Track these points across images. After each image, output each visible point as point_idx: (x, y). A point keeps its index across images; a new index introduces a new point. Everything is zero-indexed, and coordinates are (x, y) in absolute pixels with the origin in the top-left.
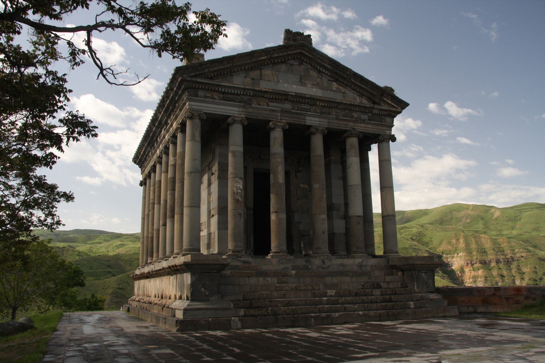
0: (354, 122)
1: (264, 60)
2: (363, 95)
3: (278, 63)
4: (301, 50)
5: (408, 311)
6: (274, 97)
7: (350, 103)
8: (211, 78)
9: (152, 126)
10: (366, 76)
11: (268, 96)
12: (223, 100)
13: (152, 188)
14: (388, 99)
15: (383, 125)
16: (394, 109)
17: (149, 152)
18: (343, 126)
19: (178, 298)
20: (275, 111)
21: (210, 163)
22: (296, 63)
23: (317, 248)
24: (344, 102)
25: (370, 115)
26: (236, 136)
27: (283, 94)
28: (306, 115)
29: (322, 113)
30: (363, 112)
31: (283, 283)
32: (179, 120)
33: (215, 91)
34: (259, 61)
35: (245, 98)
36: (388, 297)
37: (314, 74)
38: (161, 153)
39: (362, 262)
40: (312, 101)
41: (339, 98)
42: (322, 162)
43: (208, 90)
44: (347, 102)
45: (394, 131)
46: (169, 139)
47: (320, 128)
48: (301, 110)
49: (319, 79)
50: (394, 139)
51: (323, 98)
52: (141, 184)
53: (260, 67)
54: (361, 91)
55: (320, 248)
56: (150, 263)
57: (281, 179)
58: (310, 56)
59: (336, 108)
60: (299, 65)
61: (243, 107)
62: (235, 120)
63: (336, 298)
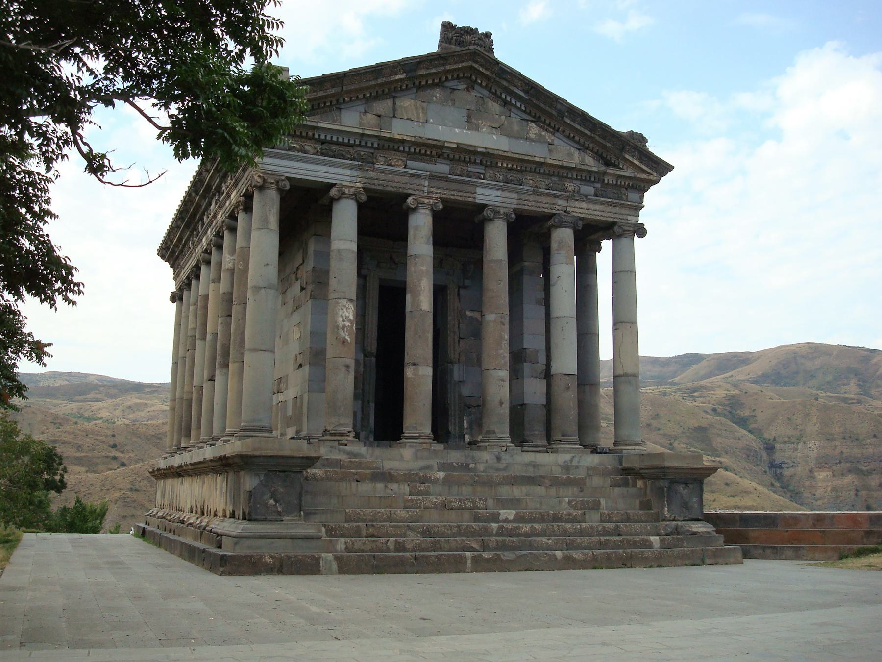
0: (567, 199)
1: (401, 80)
3: (428, 86)
4: (470, 63)
5: (647, 552)
6: (417, 151)
7: (560, 163)
9: (193, 194)
10: (593, 114)
11: (407, 149)
12: (323, 154)
13: (192, 308)
14: (633, 156)
15: (622, 206)
16: (644, 176)
17: (188, 240)
18: (547, 206)
19: (228, 516)
20: (419, 176)
21: (298, 268)
22: (462, 86)
23: (488, 432)
24: (550, 161)
25: (598, 185)
26: (345, 222)
27: (434, 146)
28: (476, 185)
29: (507, 182)
30: (585, 180)
31: (420, 493)
32: (242, 187)
33: (307, 137)
34: (391, 83)
35: (363, 152)
36: (611, 526)
37: (494, 107)
38: (209, 244)
39: (571, 461)
41: (539, 153)
42: (504, 273)
45: (643, 217)
46: (223, 222)
47: (502, 211)
48: (468, 176)
49: (503, 117)
50: (641, 231)
51: (509, 155)
52: (174, 298)
53: (394, 94)
54: (582, 140)
55: (494, 432)
56: (185, 449)
57: (425, 302)
58: (488, 73)
59: (535, 172)
61: (360, 168)
62: (344, 193)
63: (515, 525)
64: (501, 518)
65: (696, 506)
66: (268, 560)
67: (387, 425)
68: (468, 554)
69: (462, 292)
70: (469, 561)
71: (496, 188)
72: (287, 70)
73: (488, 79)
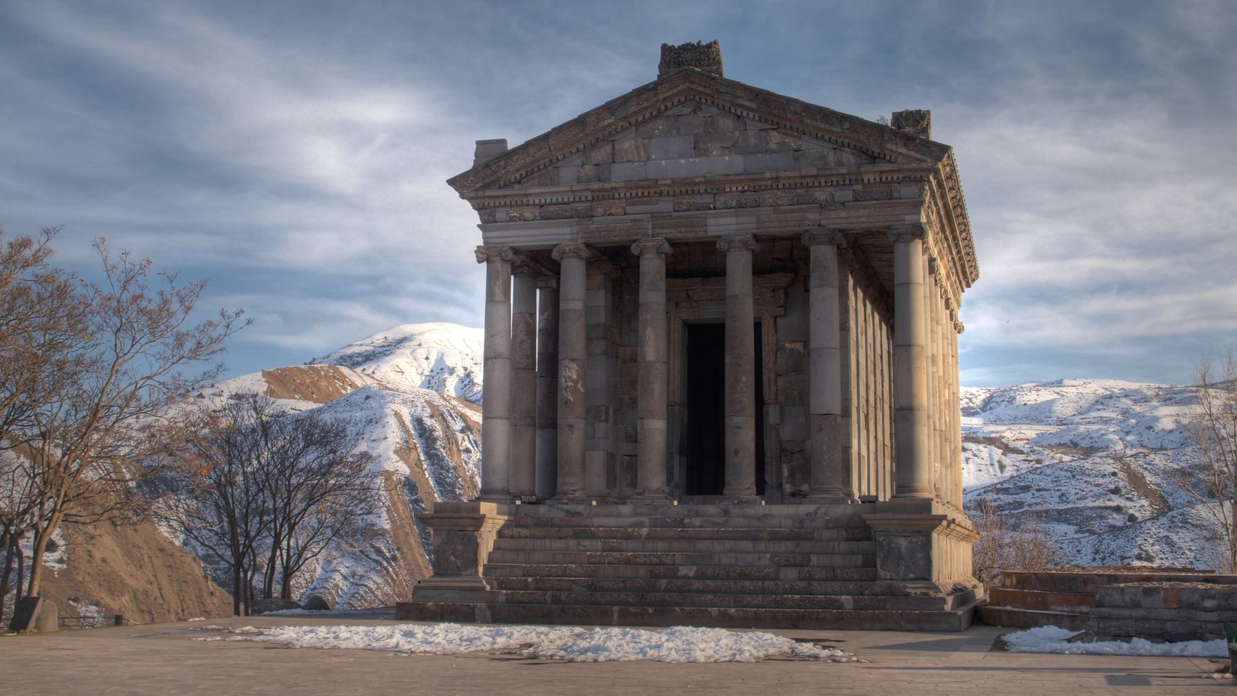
1: (610, 125)
3: (645, 121)
12: (543, 218)
14: (896, 144)
20: (641, 220)
22: (687, 110)
25: (859, 187)
31: (612, 550)
33: (522, 204)
34: (604, 128)
37: (727, 123)
39: (816, 513)
40: (714, 186)
43: (511, 206)
44: (790, 174)
47: (738, 238)
49: (737, 134)
54: (833, 138)
58: (708, 91)
60: (694, 111)
64: (680, 574)
65: (921, 562)
68: (616, 608)
69: (779, 321)
72: (503, 142)
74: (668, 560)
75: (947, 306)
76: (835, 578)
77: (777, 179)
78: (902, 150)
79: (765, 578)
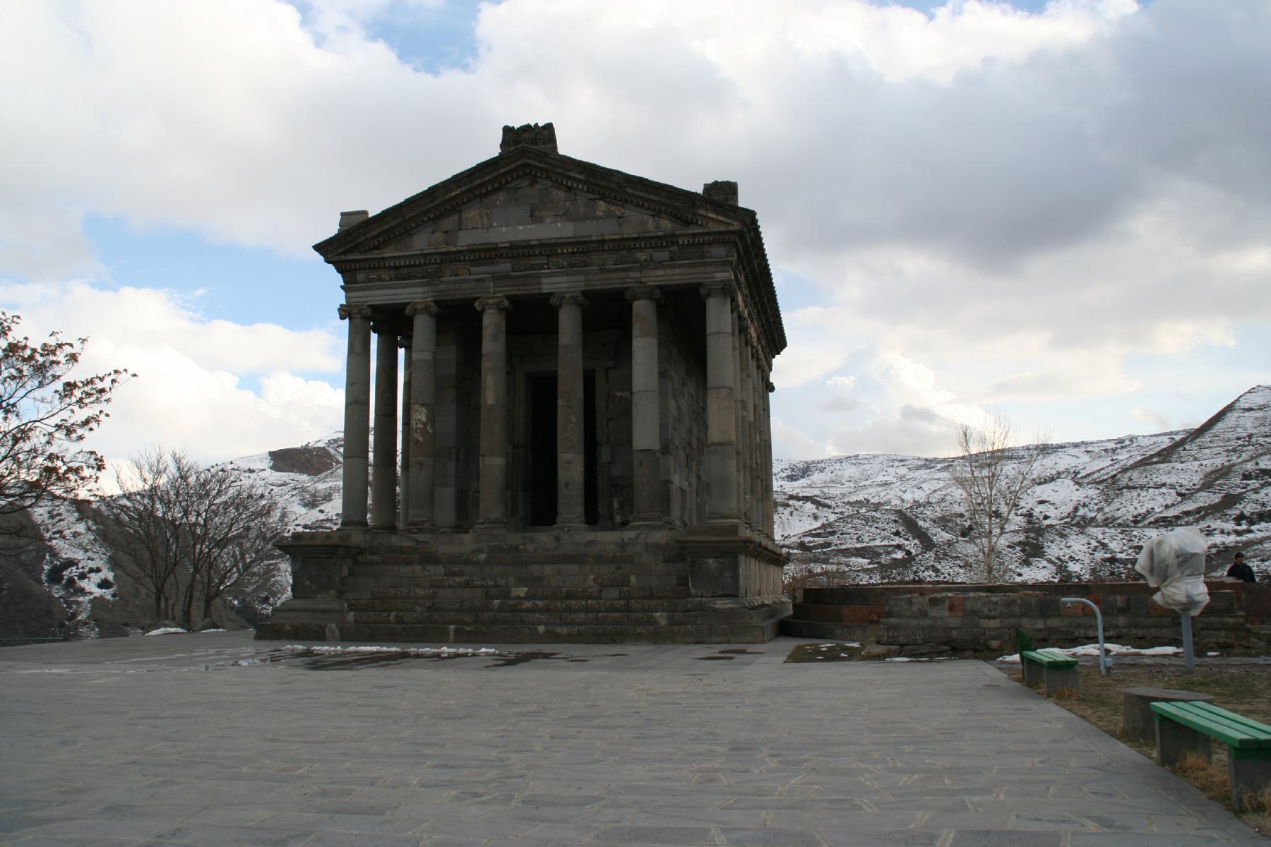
2: (660, 212)
3: (488, 194)
4: (524, 160)
7: (619, 237)
8: (377, 248)
12: (397, 279)
15: (705, 264)
16: (722, 228)
20: (482, 280)
25: (675, 248)
27: (490, 250)
28: (540, 276)
30: (656, 247)
31: (454, 574)
33: (380, 268)
35: (431, 269)
37: (559, 194)
39: (637, 538)
40: (548, 249)
47: (568, 296)
58: (543, 165)
59: (598, 250)
66: (288, 627)
67: (542, 511)
68: (452, 627)
70: (452, 633)
71: (561, 274)
72: (365, 212)
73: (547, 170)
74: (502, 582)
75: (759, 367)
76: (651, 597)
77: (603, 241)
78: (712, 215)
79: (590, 597)
